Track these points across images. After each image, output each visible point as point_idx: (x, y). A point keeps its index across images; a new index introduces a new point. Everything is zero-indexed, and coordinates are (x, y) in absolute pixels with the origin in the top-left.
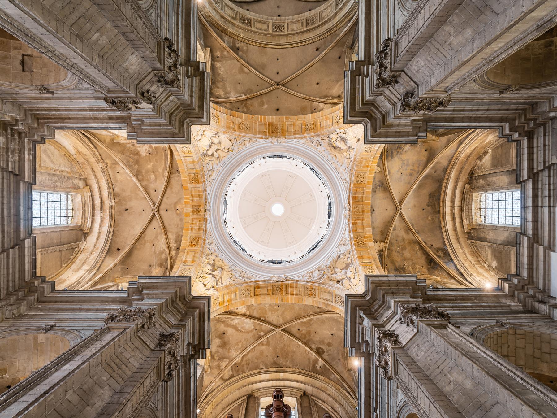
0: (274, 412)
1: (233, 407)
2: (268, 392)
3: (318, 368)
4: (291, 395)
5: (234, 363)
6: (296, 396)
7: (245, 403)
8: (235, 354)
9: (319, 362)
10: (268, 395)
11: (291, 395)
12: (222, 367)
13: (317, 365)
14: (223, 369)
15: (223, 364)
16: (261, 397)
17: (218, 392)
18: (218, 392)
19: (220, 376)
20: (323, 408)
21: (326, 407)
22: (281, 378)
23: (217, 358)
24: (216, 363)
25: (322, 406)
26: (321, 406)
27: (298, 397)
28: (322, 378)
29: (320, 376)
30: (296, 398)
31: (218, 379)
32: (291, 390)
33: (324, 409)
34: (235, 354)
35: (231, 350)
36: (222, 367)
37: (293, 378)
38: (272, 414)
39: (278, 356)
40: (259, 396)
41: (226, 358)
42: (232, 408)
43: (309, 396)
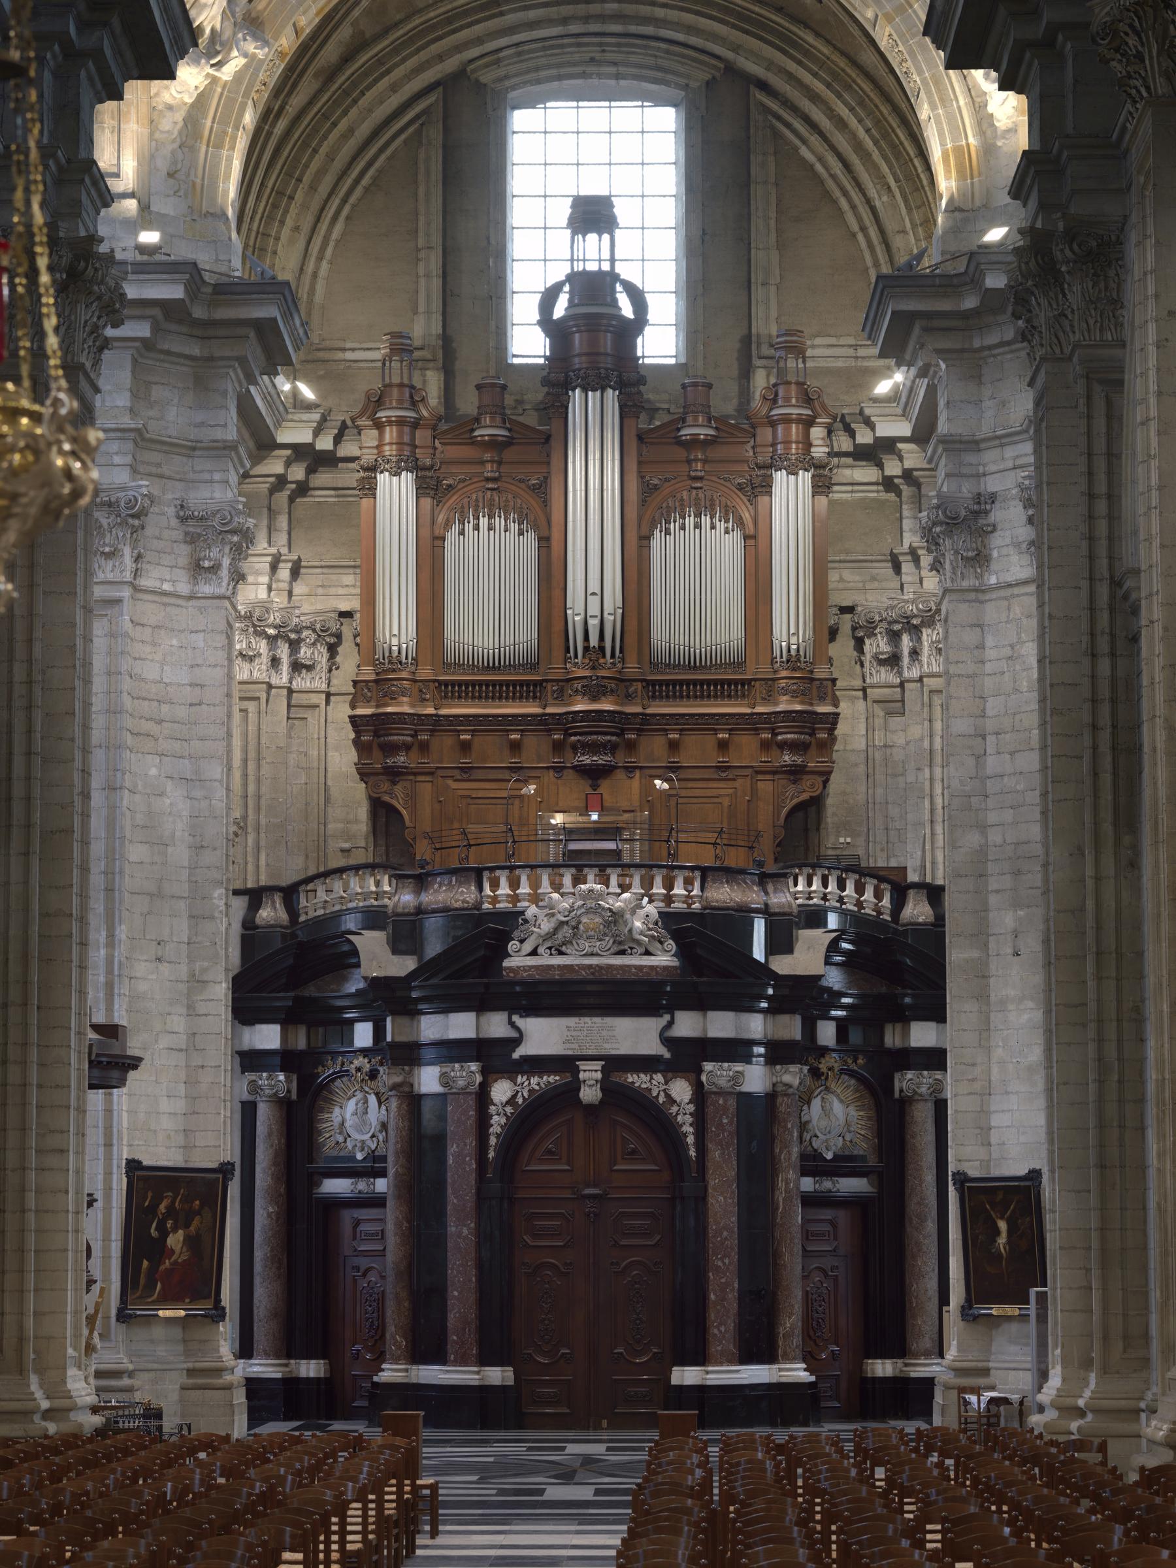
1: (383, 157)
2: (544, 61)
4: (659, 75)
6: (682, 81)
7: (435, 134)
10: (543, 74)
16: (507, 83)
17: (306, 145)
18: (306, 145)
20: (803, 160)
21: (820, 159)
25: (804, 152)
26: (796, 149)
33: (812, 167)
40: (500, 80)
42: (377, 165)
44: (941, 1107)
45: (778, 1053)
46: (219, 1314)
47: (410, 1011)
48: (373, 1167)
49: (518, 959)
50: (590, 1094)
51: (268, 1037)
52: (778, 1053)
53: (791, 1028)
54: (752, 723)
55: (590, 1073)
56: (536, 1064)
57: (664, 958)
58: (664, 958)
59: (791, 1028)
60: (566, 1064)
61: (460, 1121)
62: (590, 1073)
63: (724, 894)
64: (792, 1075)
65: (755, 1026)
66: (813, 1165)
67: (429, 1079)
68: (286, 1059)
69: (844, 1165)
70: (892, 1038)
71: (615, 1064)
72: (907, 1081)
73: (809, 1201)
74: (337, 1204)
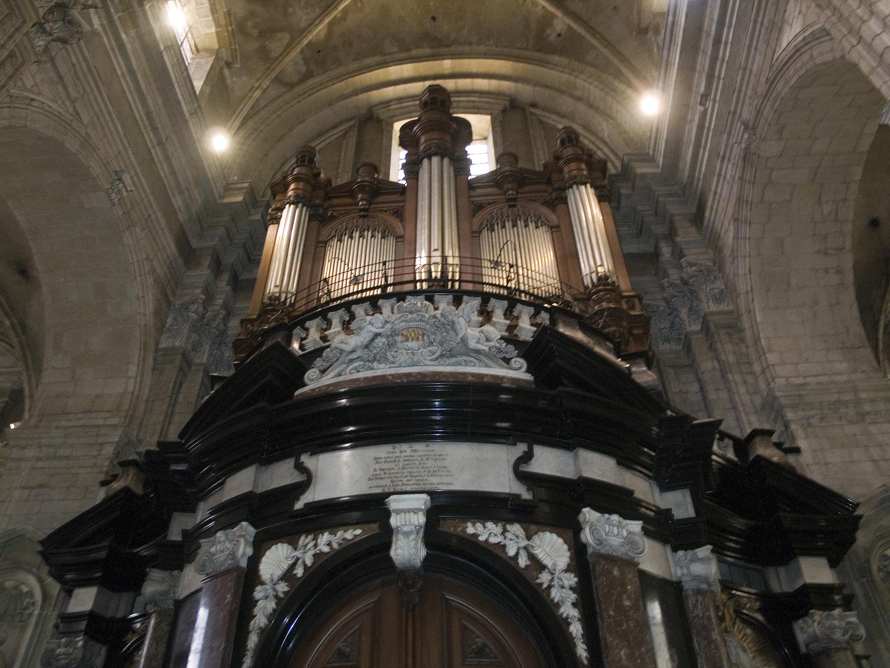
0: (423, 134)
3: (552, 37)
5: (305, 42)
8: (304, 17)
9: (555, 22)
11: (477, 110)
12: (274, 54)
13: (548, 32)
14: (276, 59)
15: (276, 46)
19: (273, 75)
22: (446, 72)
23: (255, 33)
24: (256, 45)
27: (495, 112)
28: (564, 61)
29: (556, 58)
30: (490, 114)
31: (267, 83)
32: (475, 99)
34: (304, 17)
35: (290, 10)
36: (274, 54)
37: (481, 70)
38: (418, 139)
39: (434, 18)
41: (281, 30)
43: (523, 111)
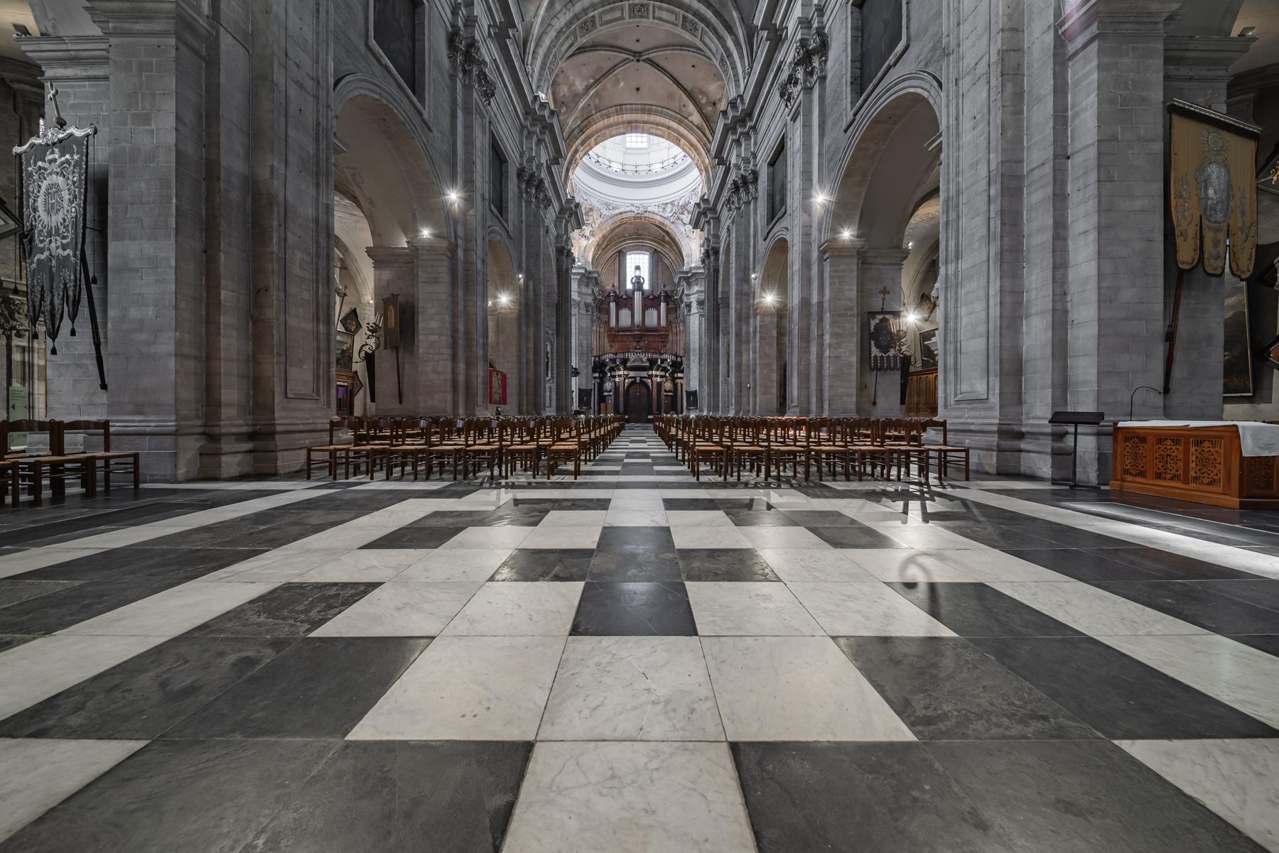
44: (682, 385)
45: (661, 377)
46: (591, 408)
47: (615, 371)
48: (610, 391)
49: (628, 364)
50: (638, 381)
51: (597, 375)
52: (661, 377)
53: (663, 373)
54: (658, 335)
55: (638, 379)
56: (631, 378)
57: (648, 364)
58: (648, 364)
59: (663, 373)
60: (635, 378)
61: (622, 384)
62: (638, 379)
63: (655, 356)
64: (664, 379)
65: (658, 373)
66: (666, 391)
67: (617, 380)
68: (599, 378)
69: (670, 391)
70: (676, 375)
71: (641, 378)
72: (679, 381)
73: (666, 396)
74: (605, 396)
